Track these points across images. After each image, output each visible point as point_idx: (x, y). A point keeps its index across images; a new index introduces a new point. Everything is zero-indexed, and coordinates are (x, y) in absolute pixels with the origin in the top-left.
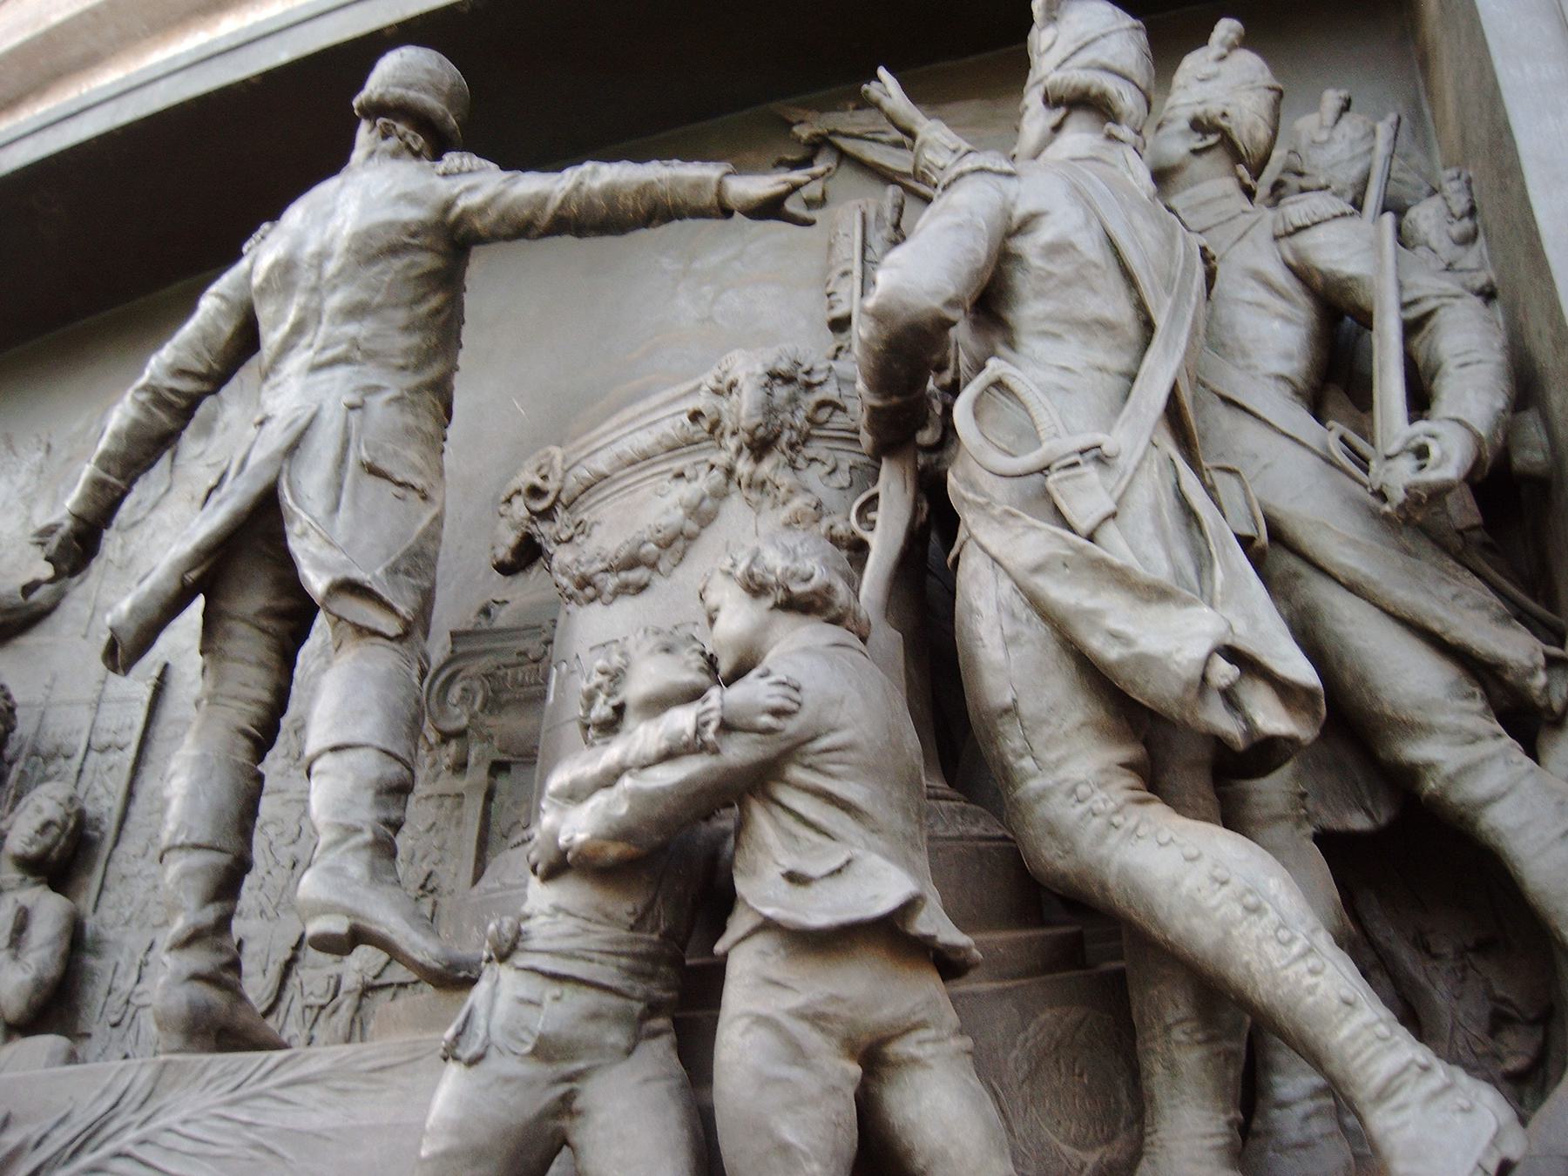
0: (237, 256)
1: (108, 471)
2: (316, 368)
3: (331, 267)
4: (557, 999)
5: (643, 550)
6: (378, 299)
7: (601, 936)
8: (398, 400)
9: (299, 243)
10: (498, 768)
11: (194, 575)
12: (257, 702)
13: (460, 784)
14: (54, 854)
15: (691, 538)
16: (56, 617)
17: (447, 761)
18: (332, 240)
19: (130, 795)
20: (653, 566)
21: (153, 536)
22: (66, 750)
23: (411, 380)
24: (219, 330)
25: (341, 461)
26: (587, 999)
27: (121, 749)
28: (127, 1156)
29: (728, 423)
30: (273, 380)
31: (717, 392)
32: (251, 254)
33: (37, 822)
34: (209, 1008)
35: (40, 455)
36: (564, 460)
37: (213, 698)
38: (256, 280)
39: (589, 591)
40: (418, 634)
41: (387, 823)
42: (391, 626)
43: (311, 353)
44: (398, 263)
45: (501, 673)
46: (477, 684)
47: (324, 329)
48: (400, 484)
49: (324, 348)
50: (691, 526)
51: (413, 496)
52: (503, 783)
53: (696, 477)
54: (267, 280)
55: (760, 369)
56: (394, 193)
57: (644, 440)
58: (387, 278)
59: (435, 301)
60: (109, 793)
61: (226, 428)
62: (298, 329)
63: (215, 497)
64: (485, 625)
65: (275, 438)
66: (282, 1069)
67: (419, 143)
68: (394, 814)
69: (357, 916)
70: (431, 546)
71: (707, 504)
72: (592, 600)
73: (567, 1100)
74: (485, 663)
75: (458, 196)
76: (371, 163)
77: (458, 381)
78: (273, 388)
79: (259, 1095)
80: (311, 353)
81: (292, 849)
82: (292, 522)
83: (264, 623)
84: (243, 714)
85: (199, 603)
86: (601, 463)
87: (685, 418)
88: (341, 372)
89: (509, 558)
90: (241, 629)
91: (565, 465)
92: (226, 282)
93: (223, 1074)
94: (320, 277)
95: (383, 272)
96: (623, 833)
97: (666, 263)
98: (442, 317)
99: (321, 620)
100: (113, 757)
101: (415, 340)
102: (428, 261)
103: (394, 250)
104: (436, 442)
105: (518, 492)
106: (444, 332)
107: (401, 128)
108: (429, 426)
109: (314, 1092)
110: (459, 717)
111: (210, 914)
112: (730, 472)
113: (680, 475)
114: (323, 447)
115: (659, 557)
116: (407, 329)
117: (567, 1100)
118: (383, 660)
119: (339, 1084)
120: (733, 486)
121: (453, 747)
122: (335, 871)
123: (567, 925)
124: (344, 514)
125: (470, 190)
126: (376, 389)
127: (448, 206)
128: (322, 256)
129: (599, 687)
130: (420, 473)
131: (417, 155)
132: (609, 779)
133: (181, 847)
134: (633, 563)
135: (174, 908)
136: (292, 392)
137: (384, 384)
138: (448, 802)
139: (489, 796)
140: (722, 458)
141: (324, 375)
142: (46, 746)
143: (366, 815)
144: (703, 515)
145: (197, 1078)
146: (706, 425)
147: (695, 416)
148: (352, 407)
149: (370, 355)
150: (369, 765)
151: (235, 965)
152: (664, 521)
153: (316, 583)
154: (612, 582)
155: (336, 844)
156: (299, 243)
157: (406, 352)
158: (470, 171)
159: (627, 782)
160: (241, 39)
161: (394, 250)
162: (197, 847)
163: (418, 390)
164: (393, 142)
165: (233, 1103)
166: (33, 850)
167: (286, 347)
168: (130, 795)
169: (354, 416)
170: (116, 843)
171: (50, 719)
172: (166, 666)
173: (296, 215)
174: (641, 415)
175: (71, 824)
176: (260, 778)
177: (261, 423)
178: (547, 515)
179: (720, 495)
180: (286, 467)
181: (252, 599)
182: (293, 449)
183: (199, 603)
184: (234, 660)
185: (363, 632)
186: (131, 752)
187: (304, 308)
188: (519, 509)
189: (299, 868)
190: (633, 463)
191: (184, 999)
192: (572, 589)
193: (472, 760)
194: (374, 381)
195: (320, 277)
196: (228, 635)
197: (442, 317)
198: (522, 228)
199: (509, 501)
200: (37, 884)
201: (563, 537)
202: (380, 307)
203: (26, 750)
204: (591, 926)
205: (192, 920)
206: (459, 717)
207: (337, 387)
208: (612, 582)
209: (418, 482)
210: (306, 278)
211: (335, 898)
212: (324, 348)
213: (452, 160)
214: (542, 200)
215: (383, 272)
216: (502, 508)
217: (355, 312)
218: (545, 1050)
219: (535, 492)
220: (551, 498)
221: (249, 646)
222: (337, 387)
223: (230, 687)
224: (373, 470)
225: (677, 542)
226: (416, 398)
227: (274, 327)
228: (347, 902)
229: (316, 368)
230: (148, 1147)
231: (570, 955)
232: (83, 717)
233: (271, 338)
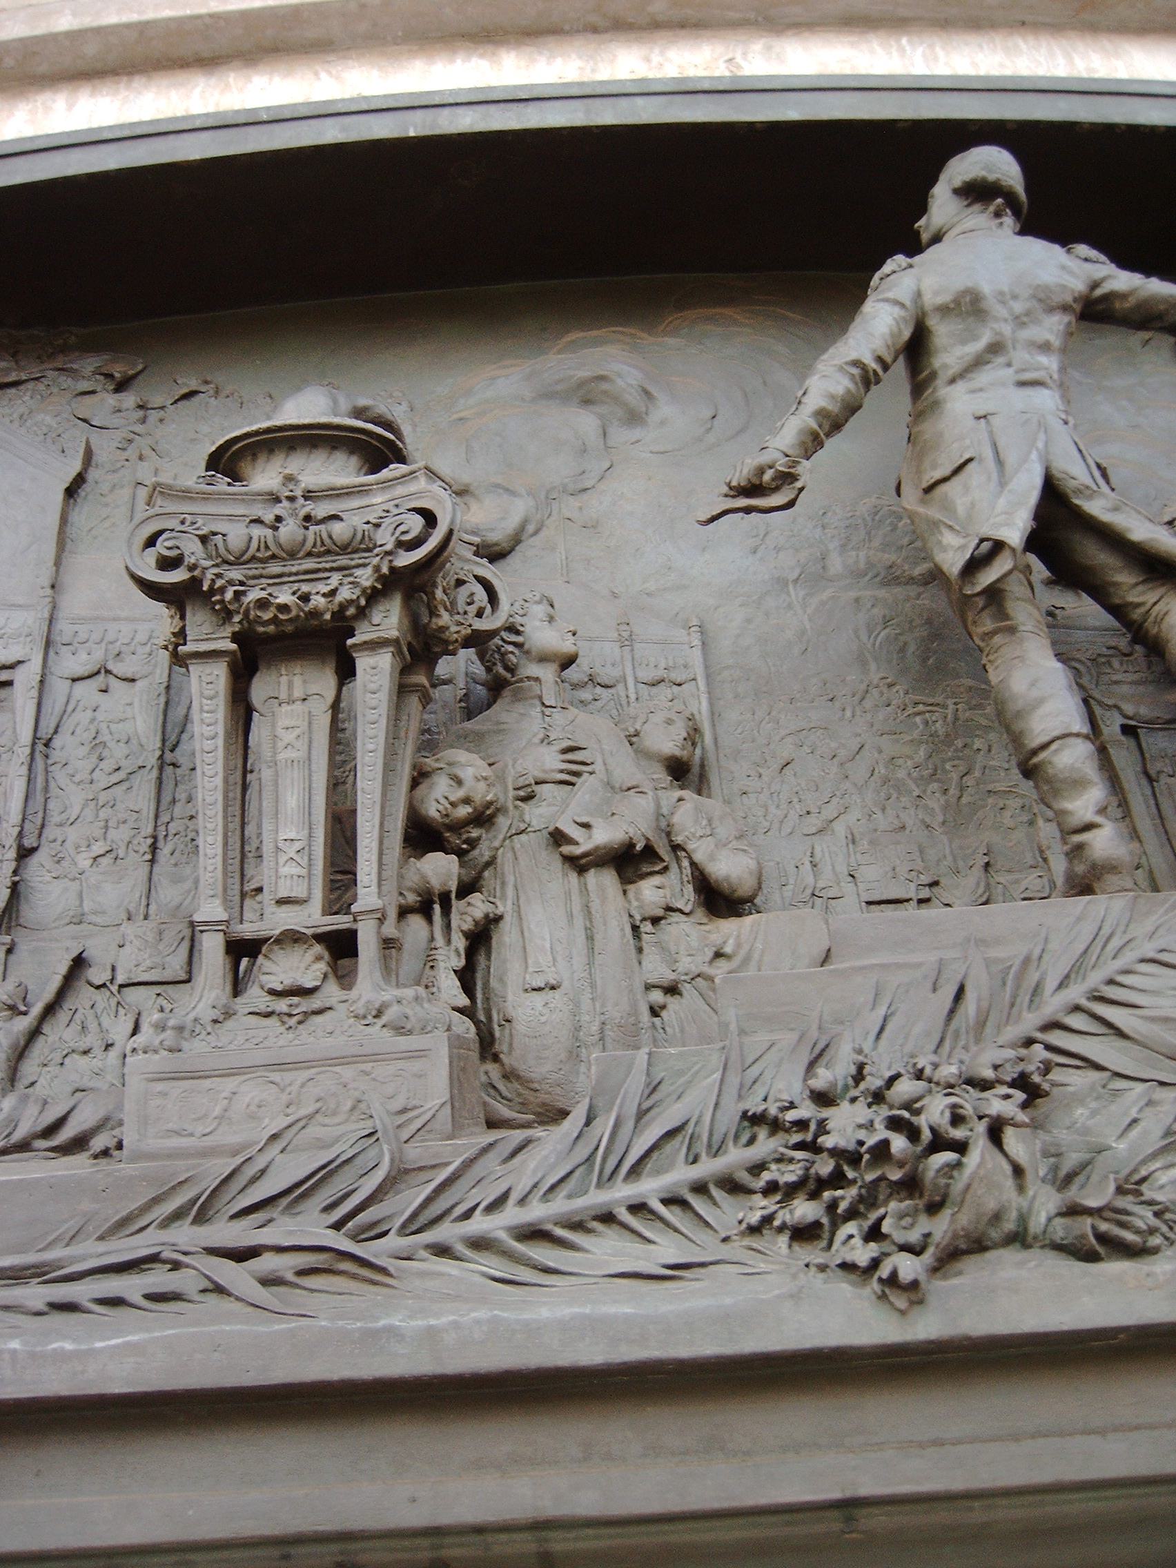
1: (820, 426)
16: (510, 559)
27: (680, 685)
75: (1104, 279)
80: (1011, 371)
127: (1095, 285)
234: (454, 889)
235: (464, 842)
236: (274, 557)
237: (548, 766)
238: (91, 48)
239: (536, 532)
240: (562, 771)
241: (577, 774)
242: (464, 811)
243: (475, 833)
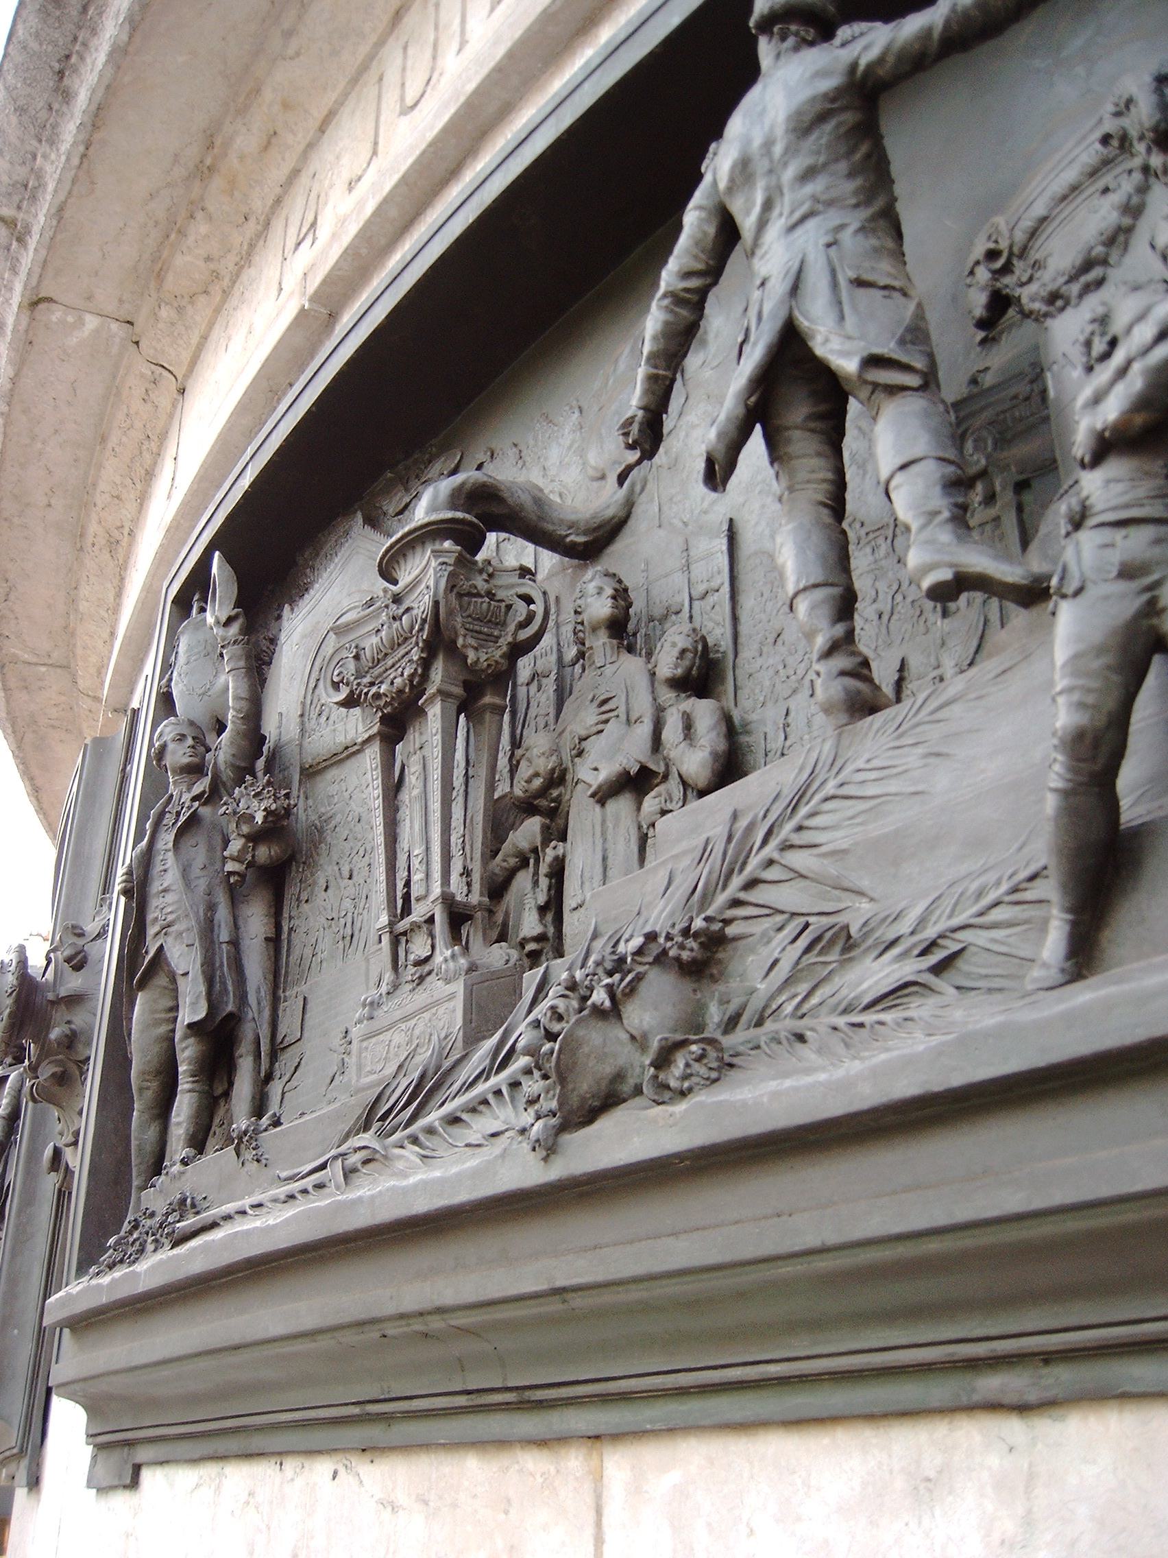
0: (699, 177)
1: (656, 367)
2: (792, 228)
3: (778, 149)
4: (1126, 537)
5: (1094, 253)
6: (822, 159)
7: (1144, 489)
8: (862, 229)
9: (747, 141)
10: (1021, 486)
11: (753, 399)
12: (824, 481)
13: (992, 512)
14: (694, 672)
15: (1129, 230)
16: (631, 522)
17: (978, 499)
18: (772, 128)
19: (735, 619)
20: (1104, 262)
21: (687, 436)
22: (673, 609)
23: (865, 213)
24: (705, 233)
25: (835, 285)
26: (1148, 532)
28: (833, 797)
29: (1134, 133)
30: (759, 252)
31: (1118, 114)
32: (712, 167)
33: (676, 652)
34: (859, 692)
35: (577, 414)
36: (1007, 223)
37: (791, 489)
38: (722, 185)
39: (1059, 303)
40: (933, 386)
41: (956, 505)
42: (912, 380)
43: (783, 220)
44: (828, 127)
45: (1002, 417)
46: (985, 433)
47: (787, 199)
48: (885, 287)
49: (792, 212)
50: (1127, 221)
51: (896, 295)
52: (1027, 497)
53: (1119, 185)
54: (732, 180)
55: (1148, 79)
56: (808, 74)
57: (1070, 175)
58: (823, 141)
59: (864, 149)
60: (718, 624)
61: (716, 336)
62: (768, 206)
63: (747, 349)
64: (975, 390)
65: (778, 288)
66: (928, 703)
67: (811, 34)
68: (960, 500)
69: (956, 565)
70: (922, 325)
71: (1135, 200)
72: (1062, 309)
73: (1152, 602)
74: (987, 415)
75: (858, 58)
76: (780, 63)
77: (900, 207)
78: (762, 257)
79: (918, 725)
80: (783, 220)
81: (875, 606)
82: (813, 337)
83: (812, 425)
84: (818, 492)
85: (758, 427)
86: (1039, 210)
87: (1098, 146)
88: (811, 224)
89: (984, 314)
90: (796, 434)
91: (1006, 228)
92: (699, 196)
93: (885, 722)
94: (771, 161)
95: (819, 138)
96: (1142, 403)
97: (1037, 63)
98: (874, 159)
99: (853, 406)
100: (711, 599)
101: (859, 182)
102: (849, 118)
103: (822, 118)
104: (899, 255)
105: (978, 263)
106: (876, 178)
107: (793, 28)
108: (890, 244)
109: (956, 709)
110: (978, 461)
111: (839, 630)
112: (1146, 169)
113: (1106, 190)
114: (817, 282)
115: (1107, 254)
116: (851, 175)
117: (1152, 602)
118: (914, 404)
119: (973, 696)
120: (1152, 180)
121: (979, 487)
122: (931, 542)
123: (1120, 487)
124: (850, 320)
125: (866, 48)
126: (842, 227)
127: (854, 66)
128: (768, 144)
129: (1092, 333)
130: (896, 278)
131: (812, 44)
132: (1123, 372)
133: (805, 589)
134: (1088, 265)
135: (810, 636)
136: (773, 256)
137: (847, 221)
138: (988, 528)
139: (1020, 509)
140: (1137, 162)
141: (799, 231)
142: (657, 612)
143: (941, 503)
144: (1134, 210)
145: (867, 734)
146: (1115, 143)
147: (1106, 140)
148: (829, 245)
149: (830, 203)
150: (930, 473)
151: (866, 663)
152: (1103, 225)
153: (848, 365)
154: (1075, 288)
155: (923, 527)
156: (747, 141)
157: (856, 192)
158: (862, 34)
159: (1137, 367)
160: (636, 24)
161: (822, 118)
162: (816, 586)
163: (873, 218)
164: (791, 41)
165: (899, 737)
166: (679, 671)
167: (762, 224)
168: (735, 619)
169: (833, 251)
170: (736, 656)
171: (654, 592)
172: (731, 520)
173: (736, 125)
174: (1059, 162)
175: (700, 648)
176: (844, 533)
177: (763, 284)
178: (1007, 269)
179: (1143, 189)
180: (794, 303)
181: (797, 412)
182: (795, 289)
183: (758, 427)
184: (798, 457)
185: (893, 390)
186: (726, 588)
187: (767, 189)
188: (983, 274)
189: (885, 617)
190: (1064, 198)
191: (840, 688)
192: (1044, 308)
193: (998, 488)
194: (837, 222)
195: (771, 161)
196: (789, 441)
197: (874, 159)
198: (918, 63)
199: (972, 273)
200: (689, 697)
201: (1024, 279)
202: (825, 165)
203: (644, 619)
204: (1136, 483)
205: (828, 636)
206: (978, 461)
207: (812, 236)
208: (1075, 288)
209: (896, 284)
210: (761, 166)
211: (937, 558)
212: (792, 212)
213: (844, 32)
214: (927, 33)
215: (819, 138)
216: (968, 281)
217: (808, 174)
218: (1127, 572)
219: (992, 255)
220: (1005, 255)
221: (803, 444)
222: (812, 236)
223: (802, 475)
224: (860, 283)
225: (1118, 238)
226: (873, 225)
227: (748, 212)
228: (947, 558)
229: (792, 228)
230: (846, 787)
231: (1127, 506)
232: (679, 580)
233: (747, 224)
234: (539, 844)
235: (553, 801)
236: (386, 655)
238: (393, 213)
239: (642, 490)
241: (606, 721)
242: (538, 782)
243: (555, 793)
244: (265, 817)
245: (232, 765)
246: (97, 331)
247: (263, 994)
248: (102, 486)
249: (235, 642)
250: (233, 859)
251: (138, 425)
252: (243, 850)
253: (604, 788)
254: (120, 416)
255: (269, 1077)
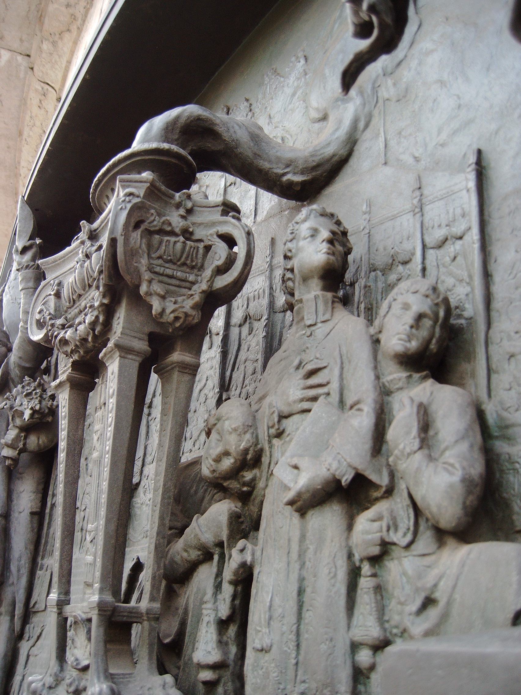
14: (433, 346)
16: (353, 162)
19: (487, 275)
21: (420, 64)
22: (401, 258)
27: (461, 238)
33: (409, 318)
35: (303, 61)
60: (461, 281)
100: (452, 248)
142: (381, 260)
166: (414, 345)
168: (487, 275)
170: (489, 325)
171: (377, 237)
172: (479, 152)
175: (442, 314)
186: (475, 234)
200: (425, 378)
203: (364, 269)
232: (408, 223)
234: (225, 539)
235: (244, 484)
237: (291, 398)
239: (367, 126)
240: (302, 400)
241: (314, 399)
242: (227, 463)
243: (248, 476)
244: (32, 416)
245: (19, 366)
246: (9, 62)
247: (23, 562)
248: (23, 163)
249: (27, 267)
250: (8, 446)
251: (38, 124)
252: (18, 437)
253: (306, 496)
254: (28, 118)
255: (21, 636)
